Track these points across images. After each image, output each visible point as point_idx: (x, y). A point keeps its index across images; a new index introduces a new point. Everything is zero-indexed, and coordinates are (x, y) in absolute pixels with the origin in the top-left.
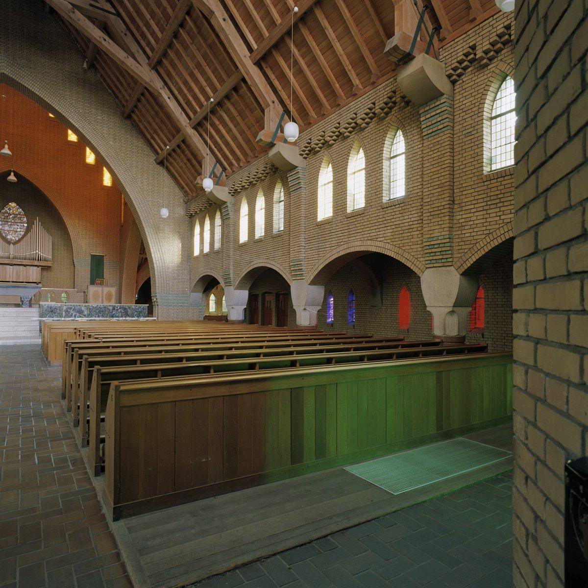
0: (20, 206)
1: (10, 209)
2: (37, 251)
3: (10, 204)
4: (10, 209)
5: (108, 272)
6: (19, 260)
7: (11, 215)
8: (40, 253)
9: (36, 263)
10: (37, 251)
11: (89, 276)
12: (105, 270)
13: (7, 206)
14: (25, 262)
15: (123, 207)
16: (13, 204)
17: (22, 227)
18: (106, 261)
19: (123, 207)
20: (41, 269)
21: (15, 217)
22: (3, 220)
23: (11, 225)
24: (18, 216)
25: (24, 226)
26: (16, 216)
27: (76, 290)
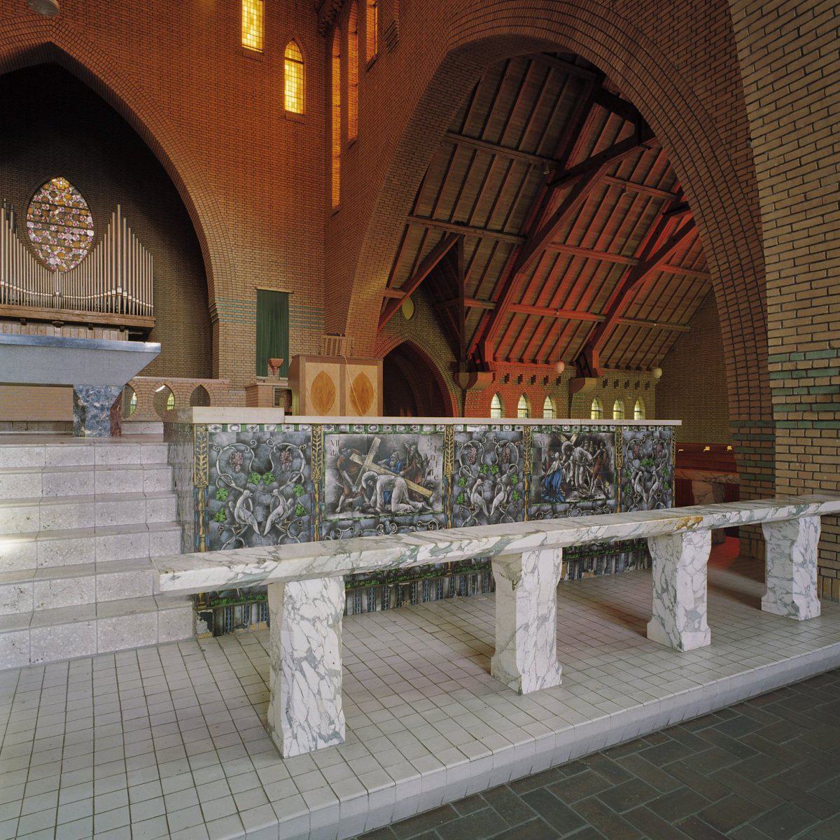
0: (76, 188)
1: (53, 194)
2: (119, 290)
3: (54, 180)
4: (53, 194)
5: (298, 340)
6: (77, 312)
7: (56, 207)
8: (125, 294)
9: (117, 320)
10: (119, 290)
11: (254, 347)
12: (291, 333)
13: (46, 186)
14: (91, 317)
15: (336, 165)
16: (61, 183)
17: (83, 238)
18: (294, 307)
19: (336, 165)
20: (129, 335)
21: (65, 214)
22: (37, 218)
23: (57, 232)
24: (74, 211)
25: (87, 236)
26: (68, 209)
27: (227, 381)
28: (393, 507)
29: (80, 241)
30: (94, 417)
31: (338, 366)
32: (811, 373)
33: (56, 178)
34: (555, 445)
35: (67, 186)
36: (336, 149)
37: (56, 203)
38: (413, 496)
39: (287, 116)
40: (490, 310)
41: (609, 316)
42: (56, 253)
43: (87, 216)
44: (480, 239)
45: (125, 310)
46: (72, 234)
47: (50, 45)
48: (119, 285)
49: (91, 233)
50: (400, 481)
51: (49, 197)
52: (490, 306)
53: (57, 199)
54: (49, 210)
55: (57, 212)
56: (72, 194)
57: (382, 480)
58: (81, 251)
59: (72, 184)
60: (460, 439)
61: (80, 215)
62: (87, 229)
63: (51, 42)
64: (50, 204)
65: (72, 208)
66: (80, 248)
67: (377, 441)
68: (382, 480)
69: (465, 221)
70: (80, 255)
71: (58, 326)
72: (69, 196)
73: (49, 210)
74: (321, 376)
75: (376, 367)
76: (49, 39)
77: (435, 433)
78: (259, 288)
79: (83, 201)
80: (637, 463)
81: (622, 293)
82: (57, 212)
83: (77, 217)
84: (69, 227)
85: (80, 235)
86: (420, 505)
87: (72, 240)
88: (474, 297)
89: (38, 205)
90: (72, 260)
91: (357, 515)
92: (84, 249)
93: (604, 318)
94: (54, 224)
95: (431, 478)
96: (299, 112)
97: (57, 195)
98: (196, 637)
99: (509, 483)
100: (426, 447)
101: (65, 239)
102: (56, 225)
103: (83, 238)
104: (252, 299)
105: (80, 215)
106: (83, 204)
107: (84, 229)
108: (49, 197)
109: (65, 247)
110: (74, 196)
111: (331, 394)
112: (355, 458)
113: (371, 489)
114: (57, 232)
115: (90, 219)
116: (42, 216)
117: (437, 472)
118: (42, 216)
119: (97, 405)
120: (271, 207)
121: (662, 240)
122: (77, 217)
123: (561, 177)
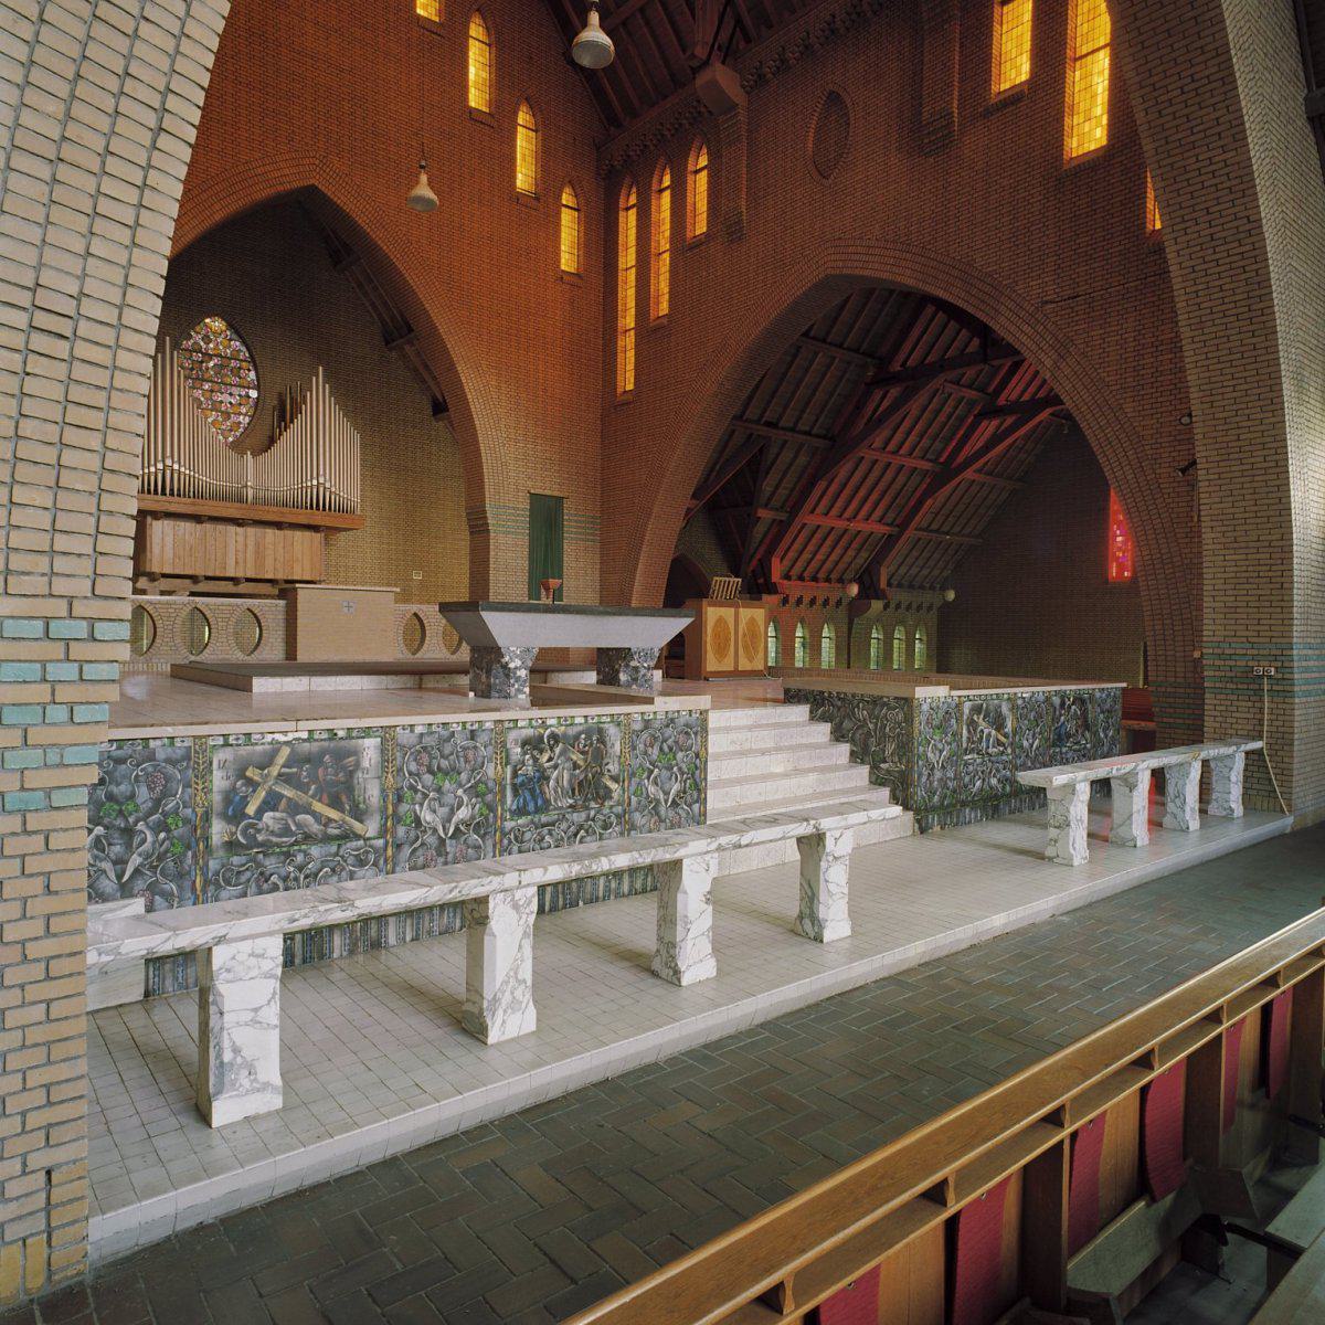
1: (207, 339)
3: (207, 320)
4: (207, 339)
7: (210, 357)
13: (198, 329)
16: (217, 324)
23: (212, 391)
26: (226, 362)
28: (990, 750)
29: (240, 404)
30: (644, 675)
31: (733, 610)
32: (1233, 657)
33: (209, 316)
34: (1063, 704)
35: (224, 328)
36: (628, 320)
37: (210, 352)
38: (999, 743)
39: (562, 277)
40: (781, 521)
41: (903, 526)
42: (210, 420)
43: (249, 370)
44: (786, 442)
45: (317, 506)
46: (231, 394)
47: (312, 191)
48: (321, 473)
49: (254, 394)
50: (994, 732)
51: (202, 343)
52: (783, 516)
53: (211, 345)
54: (202, 362)
55: (211, 364)
56: (230, 340)
57: (986, 731)
58: (242, 417)
59: (230, 326)
60: (1020, 702)
61: (240, 368)
62: (249, 388)
63: (313, 185)
64: (202, 353)
65: (230, 359)
66: (240, 414)
67: (984, 705)
68: (986, 731)
69: (774, 421)
70: (240, 423)
71: (240, 525)
72: (226, 343)
73: (202, 362)
74: (720, 621)
75: (762, 611)
76: (312, 181)
77: (1009, 699)
78: (532, 491)
79: (243, 349)
80: (1102, 716)
81: (921, 502)
82: (211, 364)
83: (236, 372)
84: (226, 384)
85: (240, 395)
86: (1001, 749)
87: (230, 403)
88: (766, 505)
89: (187, 354)
90: (231, 430)
91: (976, 756)
92: (245, 415)
93: (897, 529)
94: (208, 381)
95: (1006, 730)
96: (573, 271)
97: (210, 341)
98: (914, 835)
99: (1040, 733)
100: (1005, 709)
101: (221, 402)
102: (211, 381)
103: (243, 401)
104: (524, 505)
105: (240, 368)
106: (244, 353)
107: (244, 387)
108: (202, 343)
109: (222, 412)
110: (232, 343)
111: (727, 639)
112: (975, 717)
113: (982, 737)
114: (212, 391)
115: (252, 375)
116: (192, 369)
117: (1009, 728)
118: (192, 369)
119: (645, 665)
120: (545, 391)
121: (968, 450)
122: (236, 372)
123: (884, 379)
